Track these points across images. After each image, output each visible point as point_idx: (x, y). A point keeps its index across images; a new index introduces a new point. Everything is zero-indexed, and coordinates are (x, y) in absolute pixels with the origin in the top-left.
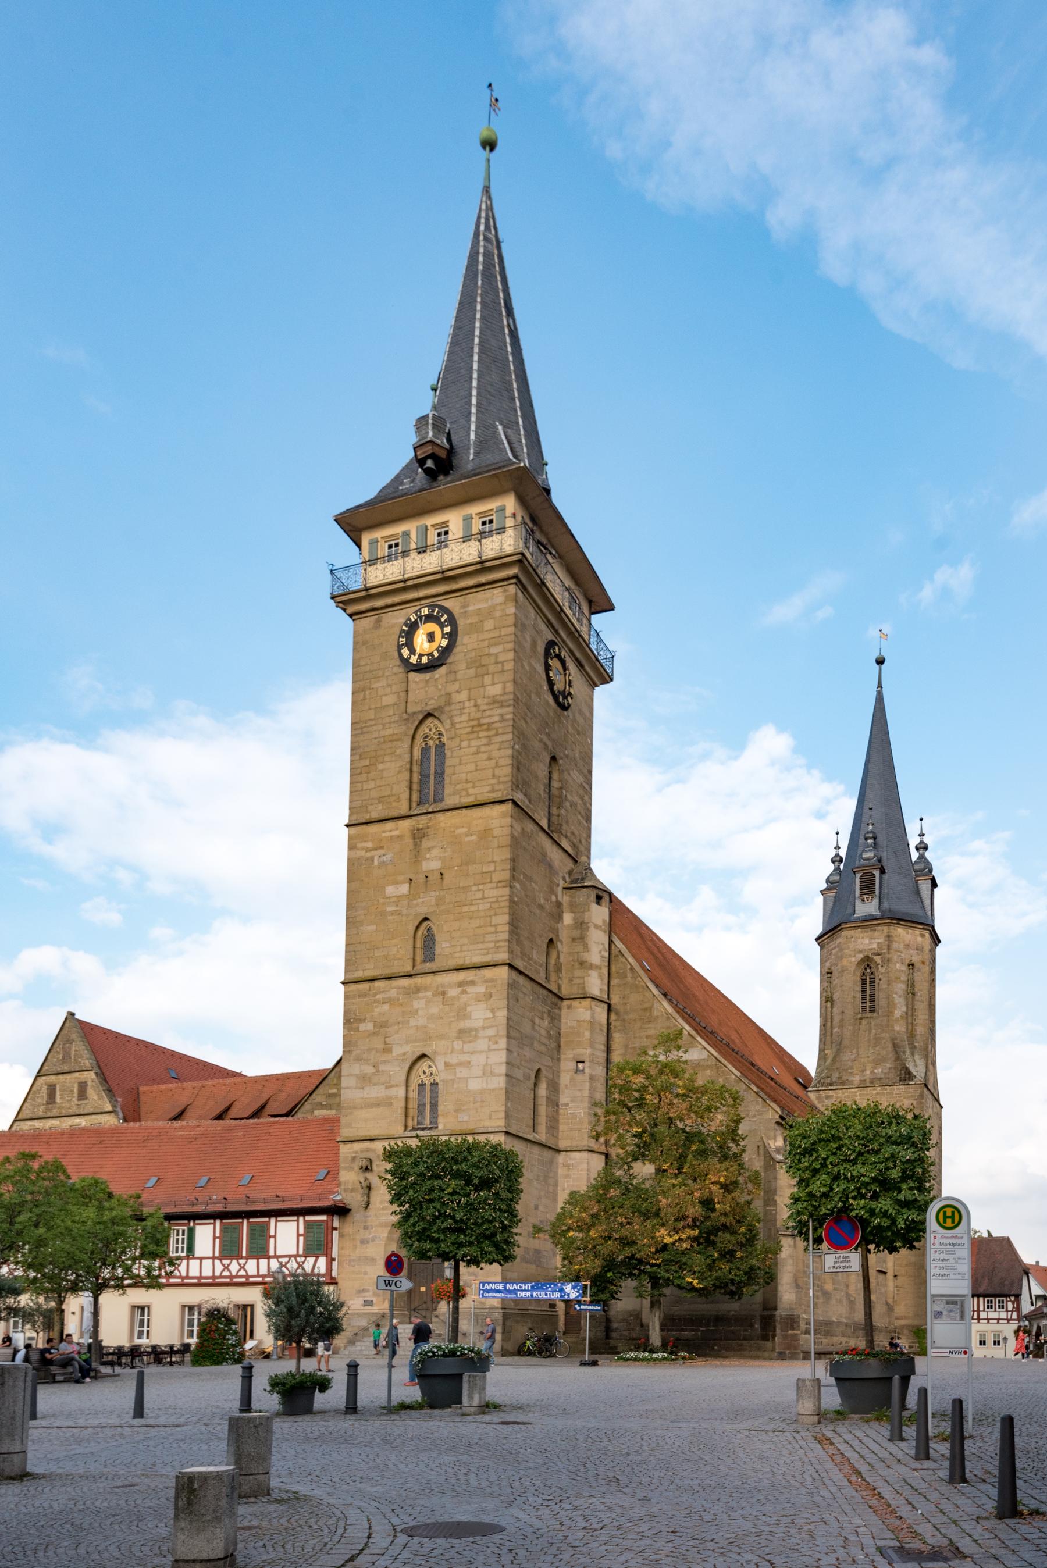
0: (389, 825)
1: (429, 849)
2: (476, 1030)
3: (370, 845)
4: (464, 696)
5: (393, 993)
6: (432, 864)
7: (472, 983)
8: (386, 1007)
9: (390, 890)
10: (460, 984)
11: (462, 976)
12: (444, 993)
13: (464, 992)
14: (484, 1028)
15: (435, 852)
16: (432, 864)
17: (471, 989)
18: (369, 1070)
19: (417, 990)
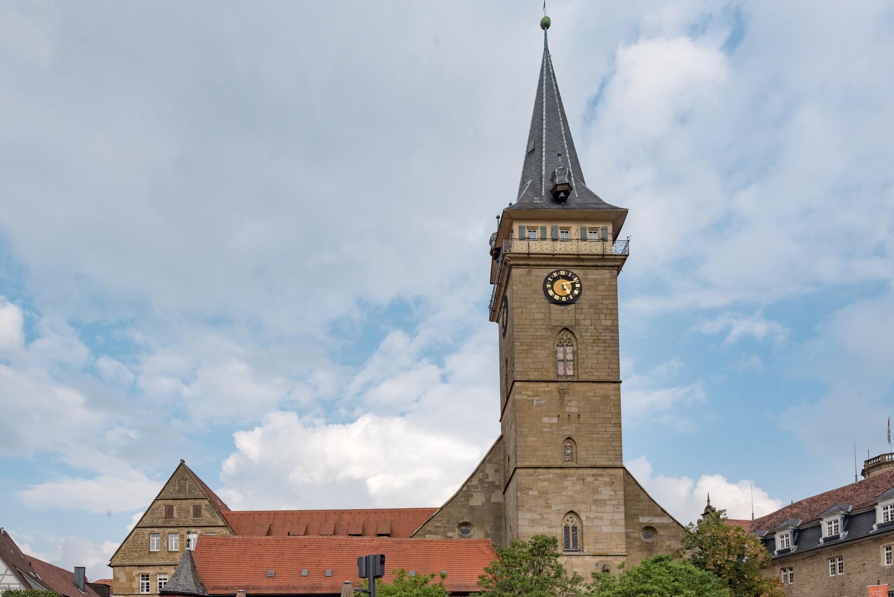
0: (543, 384)
1: (570, 401)
2: (605, 500)
3: (530, 393)
4: (588, 322)
5: (550, 476)
6: (572, 408)
7: (602, 475)
8: (546, 483)
9: (545, 420)
10: (594, 475)
11: (595, 471)
12: (583, 479)
13: (596, 480)
14: (610, 500)
15: (573, 403)
16: (572, 408)
17: (600, 479)
18: (537, 517)
19: (566, 476)
